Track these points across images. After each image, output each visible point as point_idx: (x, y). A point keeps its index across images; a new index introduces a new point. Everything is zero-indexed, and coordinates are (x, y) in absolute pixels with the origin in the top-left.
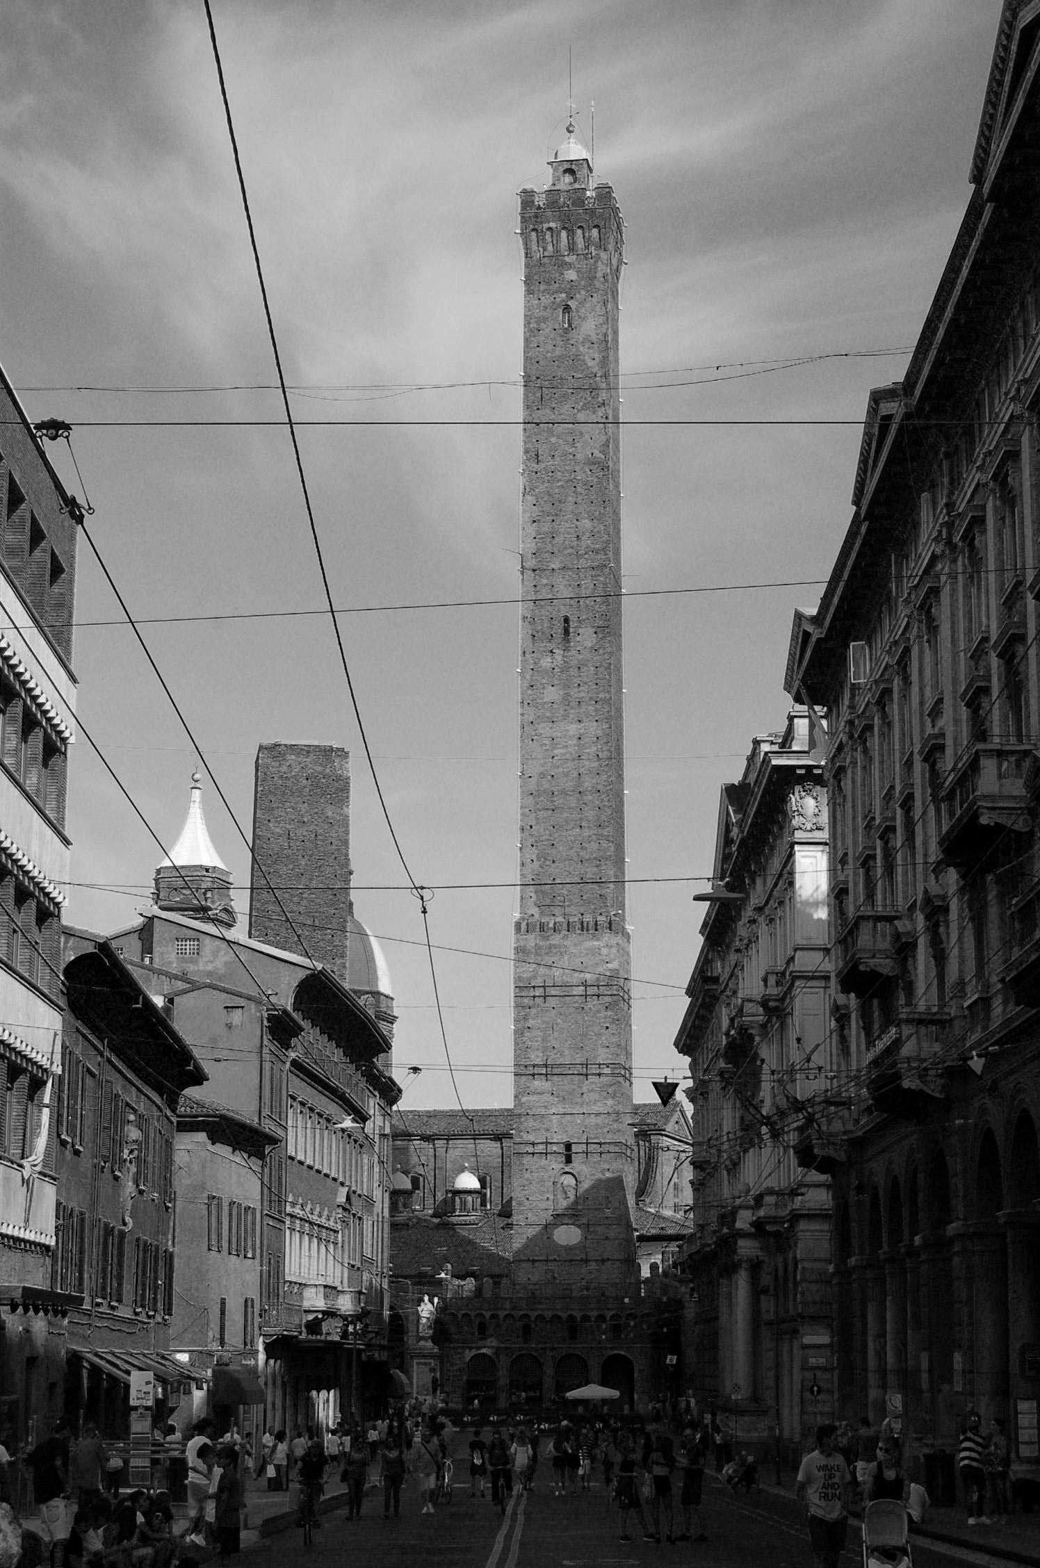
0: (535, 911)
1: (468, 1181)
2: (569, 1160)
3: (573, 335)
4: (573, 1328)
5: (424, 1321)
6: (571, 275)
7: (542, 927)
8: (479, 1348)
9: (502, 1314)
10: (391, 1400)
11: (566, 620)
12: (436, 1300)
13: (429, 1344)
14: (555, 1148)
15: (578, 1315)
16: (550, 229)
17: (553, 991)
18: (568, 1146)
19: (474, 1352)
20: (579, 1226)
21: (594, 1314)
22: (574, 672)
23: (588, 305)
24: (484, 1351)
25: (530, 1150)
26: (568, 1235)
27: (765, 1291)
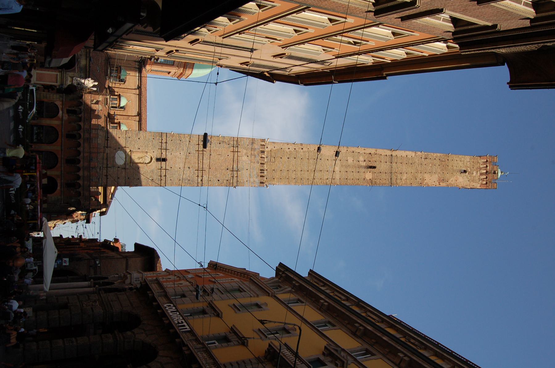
0: (269, 149)
1: (123, 103)
2: (158, 160)
3: (459, 173)
4: (73, 161)
5: (83, 81)
6: (475, 173)
7: (263, 152)
8: (62, 110)
9: (81, 124)
10: (44, 45)
11: (374, 167)
12: (95, 89)
13: (69, 83)
14: (164, 153)
15: (81, 165)
16: (487, 166)
17: (236, 155)
18: (164, 160)
19: (60, 107)
20: (125, 164)
21: (81, 173)
22: (357, 170)
23: (466, 179)
24: (61, 112)
25: (164, 141)
26: (120, 160)
27: (91, 266)
